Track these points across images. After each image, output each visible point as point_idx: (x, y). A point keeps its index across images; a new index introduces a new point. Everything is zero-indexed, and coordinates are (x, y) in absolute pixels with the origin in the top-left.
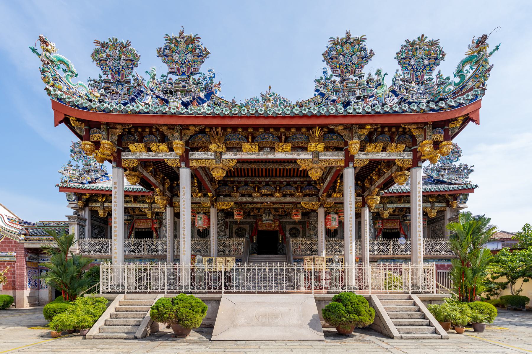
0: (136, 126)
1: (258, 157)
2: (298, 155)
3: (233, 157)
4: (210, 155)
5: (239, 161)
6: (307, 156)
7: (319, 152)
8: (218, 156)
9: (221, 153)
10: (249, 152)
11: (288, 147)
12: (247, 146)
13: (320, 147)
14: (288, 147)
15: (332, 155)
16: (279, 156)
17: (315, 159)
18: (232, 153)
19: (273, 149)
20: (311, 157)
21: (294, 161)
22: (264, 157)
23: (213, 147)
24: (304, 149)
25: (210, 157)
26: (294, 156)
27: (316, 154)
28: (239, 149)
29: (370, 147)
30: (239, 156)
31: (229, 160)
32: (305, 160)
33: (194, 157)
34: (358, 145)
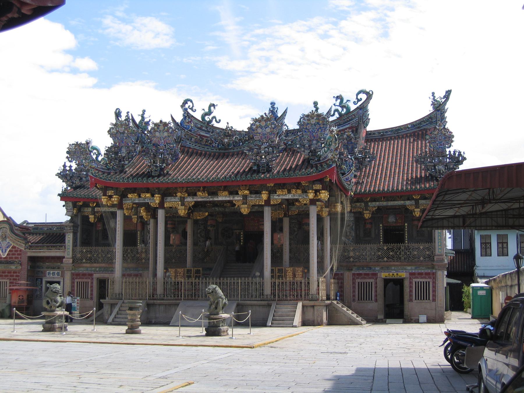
2: (233, 197)
4: (177, 199)
5: (196, 202)
6: (239, 198)
7: (247, 196)
8: (182, 200)
9: (184, 198)
10: (202, 197)
11: (226, 193)
12: (199, 193)
13: (247, 192)
14: (226, 193)
15: (256, 197)
16: (220, 199)
17: (245, 201)
18: (191, 198)
20: (242, 199)
21: (230, 202)
22: (211, 199)
23: (179, 194)
24: (237, 194)
25: (177, 200)
26: (231, 199)
27: (245, 197)
28: (195, 195)
29: (279, 192)
30: (195, 200)
32: (238, 201)
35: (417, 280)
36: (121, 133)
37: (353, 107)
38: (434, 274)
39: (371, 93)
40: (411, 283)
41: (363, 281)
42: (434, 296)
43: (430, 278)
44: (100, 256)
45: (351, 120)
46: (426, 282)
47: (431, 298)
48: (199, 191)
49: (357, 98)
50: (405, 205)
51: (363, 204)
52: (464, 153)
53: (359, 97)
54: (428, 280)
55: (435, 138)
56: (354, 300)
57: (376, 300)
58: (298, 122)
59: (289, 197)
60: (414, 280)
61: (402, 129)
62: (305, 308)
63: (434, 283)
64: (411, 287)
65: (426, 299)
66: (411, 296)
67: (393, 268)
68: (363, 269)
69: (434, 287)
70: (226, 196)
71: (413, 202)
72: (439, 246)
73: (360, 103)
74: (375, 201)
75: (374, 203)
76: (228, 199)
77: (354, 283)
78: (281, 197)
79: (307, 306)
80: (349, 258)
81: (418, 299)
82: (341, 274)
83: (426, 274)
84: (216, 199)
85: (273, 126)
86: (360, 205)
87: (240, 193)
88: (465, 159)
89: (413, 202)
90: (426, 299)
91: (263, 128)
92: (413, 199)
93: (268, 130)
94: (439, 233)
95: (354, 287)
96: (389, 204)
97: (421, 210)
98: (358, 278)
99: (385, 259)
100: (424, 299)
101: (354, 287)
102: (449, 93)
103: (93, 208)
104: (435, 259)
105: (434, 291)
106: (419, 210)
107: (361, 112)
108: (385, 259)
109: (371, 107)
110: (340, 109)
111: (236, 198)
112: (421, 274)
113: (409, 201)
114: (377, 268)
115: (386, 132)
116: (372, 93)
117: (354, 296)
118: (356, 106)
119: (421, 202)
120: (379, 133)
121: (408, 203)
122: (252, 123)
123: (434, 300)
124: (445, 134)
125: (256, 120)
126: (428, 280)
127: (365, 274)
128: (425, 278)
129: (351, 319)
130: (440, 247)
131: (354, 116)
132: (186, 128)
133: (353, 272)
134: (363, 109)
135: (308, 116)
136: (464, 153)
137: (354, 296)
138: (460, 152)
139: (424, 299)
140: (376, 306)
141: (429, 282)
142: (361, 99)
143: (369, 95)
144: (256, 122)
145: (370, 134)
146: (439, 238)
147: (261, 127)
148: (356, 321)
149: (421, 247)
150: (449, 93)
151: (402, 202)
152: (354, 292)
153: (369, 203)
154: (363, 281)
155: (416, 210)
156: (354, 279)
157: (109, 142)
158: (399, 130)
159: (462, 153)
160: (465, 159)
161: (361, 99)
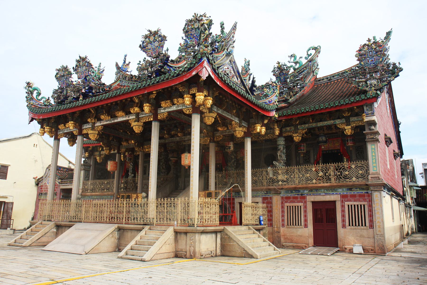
0: (59, 116)
1: (110, 122)
2: (129, 117)
3: (100, 124)
9: (94, 123)
10: (106, 120)
16: (120, 120)
18: (99, 122)
19: (115, 117)
20: (135, 117)
22: (113, 122)
26: (127, 118)
30: (102, 124)
31: (98, 126)
33: (84, 128)
34: (179, 99)
35: (350, 203)
36: (62, 76)
37: (304, 61)
38: (370, 196)
39: (319, 48)
40: (343, 206)
41: (292, 204)
42: (371, 221)
43: (365, 200)
44: (97, 187)
45: (304, 71)
46: (361, 205)
47: (367, 224)
48: (103, 114)
49: (308, 54)
50: (336, 125)
51: (293, 128)
52: (399, 63)
53: (309, 53)
54: (362, 203)
55: (365, 55)
56: (283, 225)
57: (306, 226)
58: (184, 30)
59: (174, 108)
60: (347, 203)
61: (347, 72)
62: (179, 234)
63: (370, 206)
64: (343, 211)
65: (362, 225)
66: (343, 221)
67: (323, 190)
68: (292, 192)
69: (371, 211)
70: (122, 116)
71: (344, 120)
72: (373, 163)
73: (310, 57)
74: (305, 123)
75: (303, 126)
76: (124, 119)
77: (283, 207)
78: (167, 110)
79: (180, 233)
80: (278, 181)
81: (353, 225)
82: (270, 197)
83: (360, 196)
84: (116, 121)
85: (160, 39)
86: (290, 129)
87: (132, 111)
88: (401, 70)
89: (344, 120)
90: (362, 225)
91: (153, 43)
92: (344, 117)
93: (156, 44)
94: (372, 149)
95: (283, 212)
96: (319, 126)
97: (352, 127)
98: (286, 202)
99: (314, 181)
100: (359, 225)
101: (283, 212)
102: (389, 33)
103: (100, 152)
104: (370, 178)
105: (371, 216)
106: (350, 127)
107: (310, 64)
108: (314, 181)
109: (320, 60)
110: (294, 65)
111: (131, 118)
112: (353, 196)
113: (339, 120)
114: (306, 192)
115: (333, 77)
116: (320, 47)
117: (283, 220)
118: (307, 61)
119: (352, 119)
120: (327, 78)
121: (338, 122)
122: (143, 40)
123: (372, 226)
124: (375, 49)
125: (146, 37)
126: (362, 203)
127: (294, 198)
128: (359, 201)
129: (245, 250)
130: (374, 165)
131: (305, 68)
132: (124, 70)
133: (282, 195)
134: (311, 61)
135: (191, 21)
136: (399, 63)
137: (283, 220)
138: (394, 64)
139: (359, 225)
140: (307, 232)
141: (364, 205)
142: (311, 54)
143: (317, 49)
144: (146, 39)
145: (319, 80)
146: (373, 154)
147: (151, 43)
148: (250, 253)
149: (353, 166)
150: (389, 33)
151: (332, 122)
152: (283, 216)
153: (299, 127)
154: (292, 204)
155: (346, 127)
156: (282, 203)
157: (56, 85)
158: (344, 73)
159: (397, 64)
160: (401, 70)
161: (311, 54)
